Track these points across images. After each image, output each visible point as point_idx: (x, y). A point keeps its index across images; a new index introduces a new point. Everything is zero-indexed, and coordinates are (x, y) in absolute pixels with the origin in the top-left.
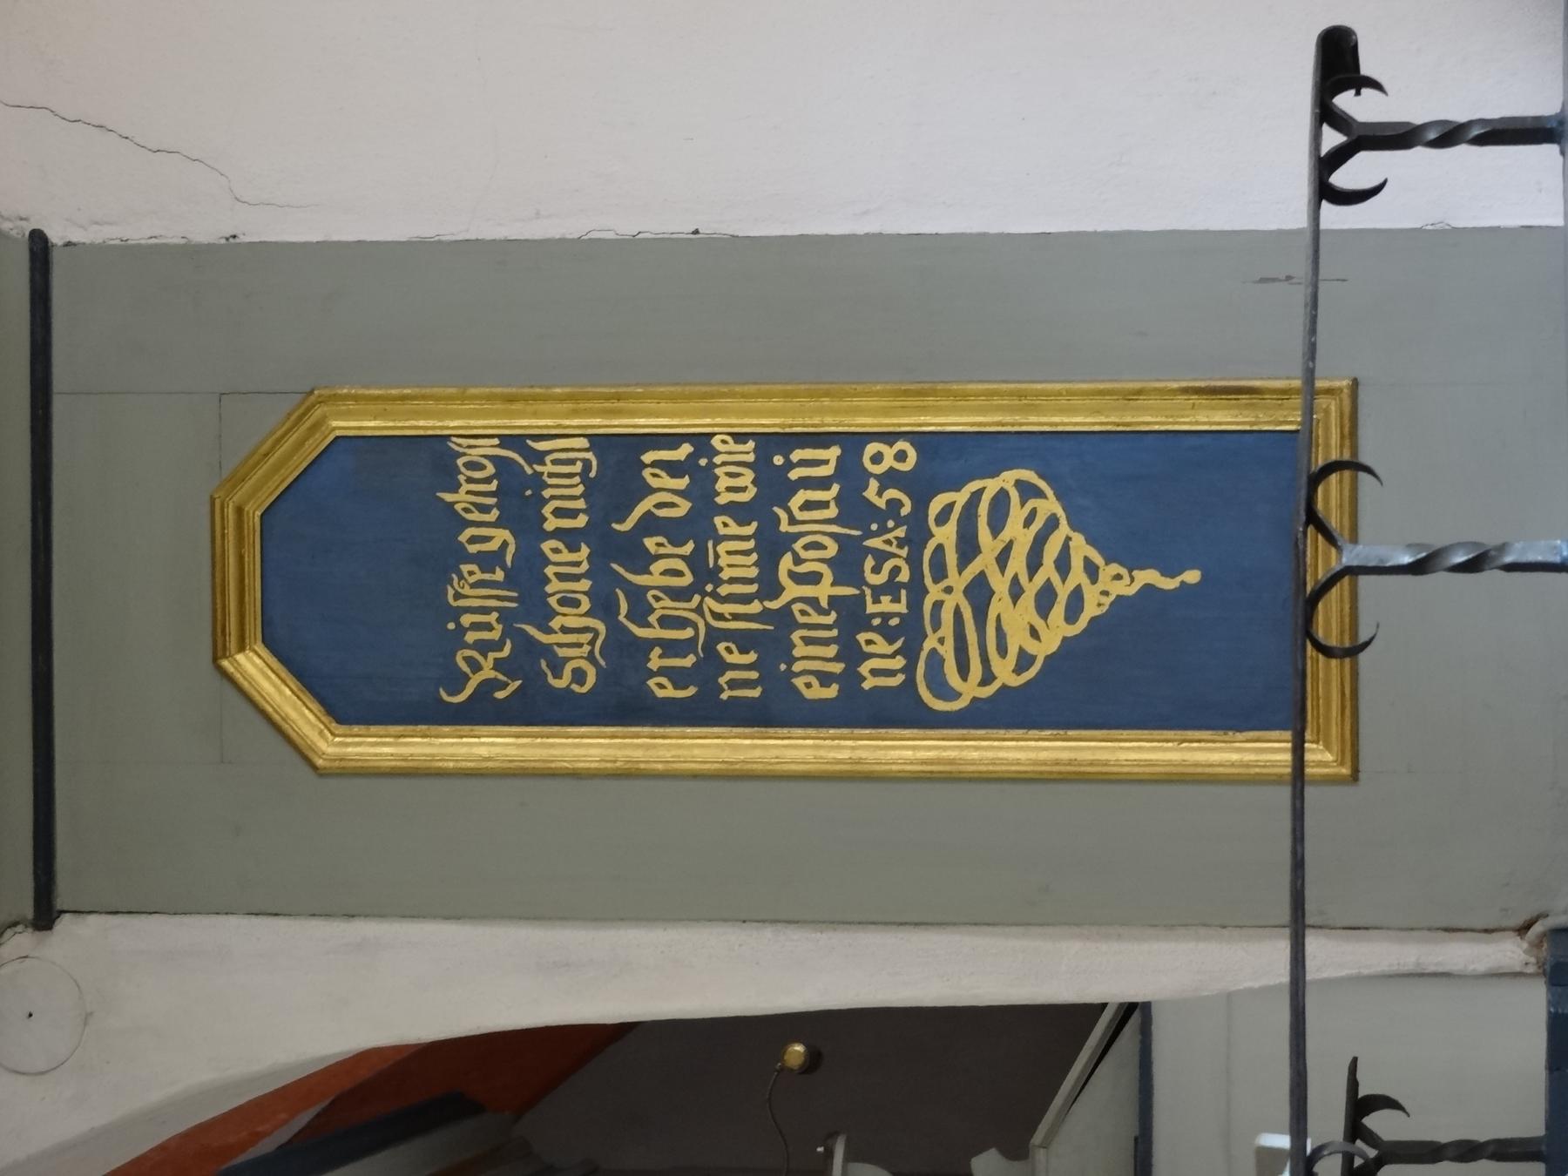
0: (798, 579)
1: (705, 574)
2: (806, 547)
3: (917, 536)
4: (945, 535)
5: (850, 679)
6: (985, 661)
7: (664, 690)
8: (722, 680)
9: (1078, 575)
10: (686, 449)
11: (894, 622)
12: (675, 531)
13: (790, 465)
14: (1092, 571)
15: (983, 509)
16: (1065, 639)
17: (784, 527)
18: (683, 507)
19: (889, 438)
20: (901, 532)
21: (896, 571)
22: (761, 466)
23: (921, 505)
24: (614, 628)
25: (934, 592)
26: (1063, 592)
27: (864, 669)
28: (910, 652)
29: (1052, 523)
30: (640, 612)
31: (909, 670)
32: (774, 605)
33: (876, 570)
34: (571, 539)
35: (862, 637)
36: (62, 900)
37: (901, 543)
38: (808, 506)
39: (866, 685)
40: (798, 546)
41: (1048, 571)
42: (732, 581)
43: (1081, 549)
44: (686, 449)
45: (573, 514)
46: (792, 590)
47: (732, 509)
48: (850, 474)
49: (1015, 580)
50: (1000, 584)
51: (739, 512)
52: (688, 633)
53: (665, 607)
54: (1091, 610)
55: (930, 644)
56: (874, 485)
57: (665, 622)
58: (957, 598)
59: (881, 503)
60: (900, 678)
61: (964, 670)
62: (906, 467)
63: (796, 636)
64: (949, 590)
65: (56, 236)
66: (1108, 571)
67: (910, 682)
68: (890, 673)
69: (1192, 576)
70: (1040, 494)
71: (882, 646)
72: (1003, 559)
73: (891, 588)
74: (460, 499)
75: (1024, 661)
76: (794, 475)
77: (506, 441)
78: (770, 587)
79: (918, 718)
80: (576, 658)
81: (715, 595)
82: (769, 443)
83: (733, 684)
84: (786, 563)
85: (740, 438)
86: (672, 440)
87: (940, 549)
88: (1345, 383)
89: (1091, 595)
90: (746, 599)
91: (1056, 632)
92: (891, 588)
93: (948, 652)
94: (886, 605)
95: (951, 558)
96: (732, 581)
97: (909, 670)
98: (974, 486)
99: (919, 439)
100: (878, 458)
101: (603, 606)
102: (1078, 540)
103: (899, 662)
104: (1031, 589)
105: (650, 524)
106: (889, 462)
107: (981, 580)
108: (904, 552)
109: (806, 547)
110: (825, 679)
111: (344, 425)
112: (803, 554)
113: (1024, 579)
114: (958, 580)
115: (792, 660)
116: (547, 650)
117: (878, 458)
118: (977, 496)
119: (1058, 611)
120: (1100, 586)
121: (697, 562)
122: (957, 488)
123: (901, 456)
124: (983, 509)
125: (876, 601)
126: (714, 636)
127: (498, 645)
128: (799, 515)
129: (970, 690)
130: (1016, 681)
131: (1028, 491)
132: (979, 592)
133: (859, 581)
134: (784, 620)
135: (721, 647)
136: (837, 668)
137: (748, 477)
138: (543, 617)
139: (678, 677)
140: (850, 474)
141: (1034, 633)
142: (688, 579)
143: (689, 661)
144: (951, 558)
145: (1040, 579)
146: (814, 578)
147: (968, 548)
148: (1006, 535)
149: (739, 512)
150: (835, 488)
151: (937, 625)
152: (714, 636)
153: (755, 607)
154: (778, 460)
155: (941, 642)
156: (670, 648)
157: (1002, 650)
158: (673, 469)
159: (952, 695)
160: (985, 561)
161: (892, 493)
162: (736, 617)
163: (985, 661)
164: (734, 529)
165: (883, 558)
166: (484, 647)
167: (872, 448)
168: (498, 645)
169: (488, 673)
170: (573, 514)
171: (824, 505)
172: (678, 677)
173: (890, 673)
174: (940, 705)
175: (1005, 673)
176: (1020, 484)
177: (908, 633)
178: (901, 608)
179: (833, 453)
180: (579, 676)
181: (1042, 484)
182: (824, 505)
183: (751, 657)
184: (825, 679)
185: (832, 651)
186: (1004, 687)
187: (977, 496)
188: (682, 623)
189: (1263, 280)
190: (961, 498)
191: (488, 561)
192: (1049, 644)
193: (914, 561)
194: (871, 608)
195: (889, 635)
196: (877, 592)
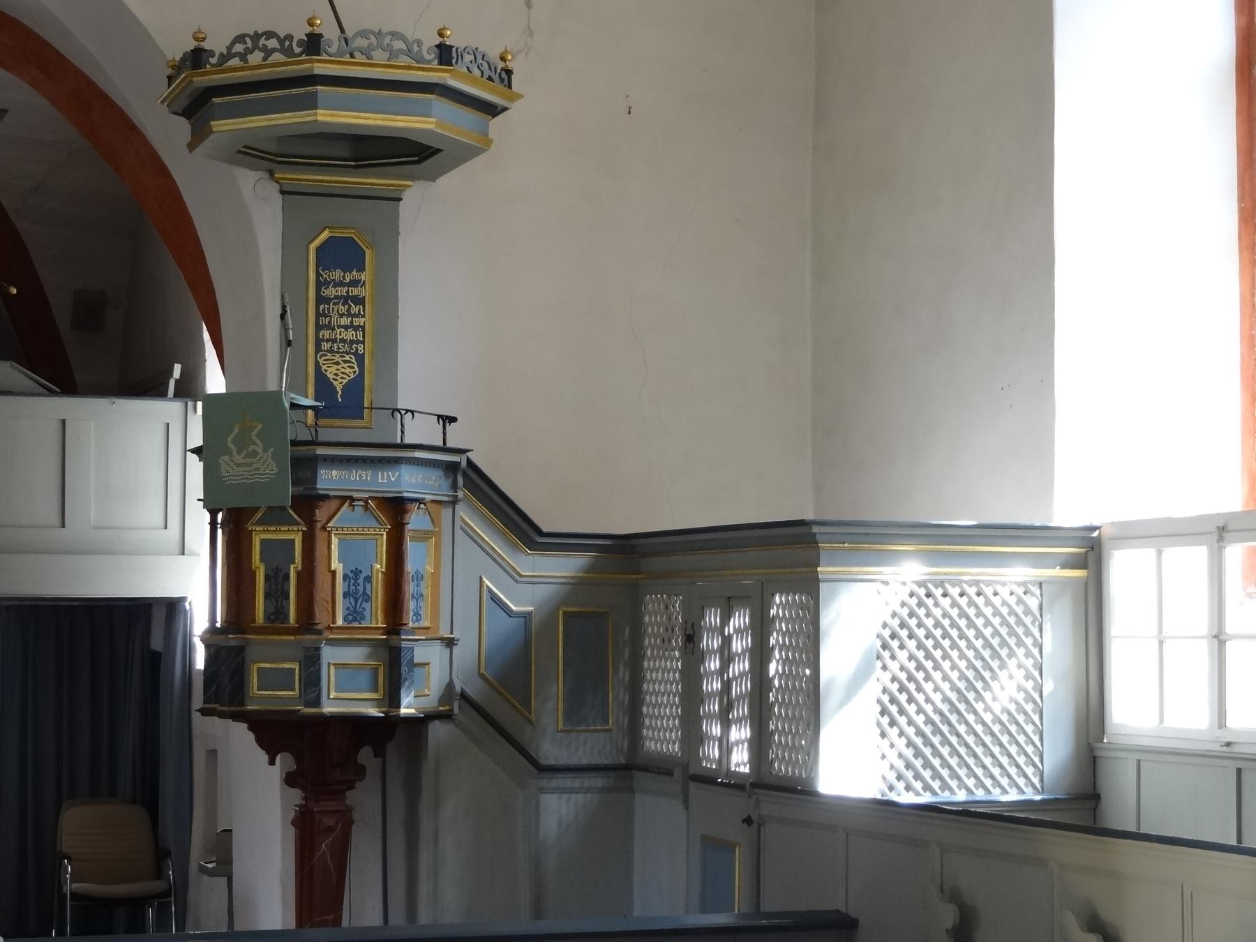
1: (341, 316)
4: (347, 358)
5: (323, 340)
7: (321, 307)
9: (340, 380)
10: (363, 313)
12: (349, 311)
14: (341, 383)
18: (353, 313)
19: (364, 349)
22: (359, 326)
23: (352, 354)
24: (333, 299)
25: (338, 356)
27: (325, 343)
28: (328, 351)
29: (349, 376)
30: (334, 304)
31: (325, 351)
34: (347, 292)
36: (286, 196)
38: (353, 335)
41: (341, 375)
43: (345, 381)
44: (363, 313)
45: (352, 293)
47: (352, 321)
48: (358, 342)
50: (339, 367)
51: (352, 321)
52: (331, 312)
53: (336, 308)
55: (329, 354)
57: (333, 308)
58: (337, 360)
61: (324, 360)
63: (331, 331)
65: (401, 202)
66: (341, 385)
69: (340, 400)
71: (329, 346)
73: (339, 348)
74: (354, 272)
75: (326, 371)
77: (364, 281)
78: (339, 327)
79: (316, 353)
80: (327, 292)
82: (363, 328)
84: (343, 330)
85: (364, 323)
86: (364, 311)
90: (337, 323)
91: (331, 376)
92: (339, 348)
93: (327, 358)
94: (336, 347)
97: (325, 351)
100: (360, 347)
101: (336, 297)
102: (347, 381)
104: (338, 372)
105: (350, 306)
106: (360, 349)
110: (323, 336)
111: (368, 253)
114: (340, 360)
115: (327, 330)
116: (328, 287)
118: (354, 364)
119: (335, 377)
121: (343, 314)
122: (356, 360)
123: (361, 351)
126: (331, 317)
127: (329, 278)
129: (321, 361)
130: (323, 369)
131: (355, 372)
132: (337, 363)
134: (333, 329)
138: (334, 286)
139: (324, 310)
140: (358, 342)
142: (340, 313)
143: (326, 312)
146: (340, 335)
147: (345, 362)
148: (347, 368)
149: (352, 321)
152: (331, 317)
153: (336, 324)
155: (329, 356)
156: (329, 309)
157: (328, 367)
158: (359, 311)
159: (320, 358)
160: (343, 365)
164: (349, 321)
165: (344, 347)
166: (329, 276)
167: (362, 346)
168: (329, 278)
169: (325, 276)
170: (352, 293)
172: (324, 310)
174: (318, 356)
175: (324, 367)
177: (331, 351)
178: (335, 350)
179: (361, 339)
180: (324, 292)
184: (323, 336)
187: (354, 364)
188: (333, 311)
190: (354, 361)
191: (344, 279)
192: (328, 374)
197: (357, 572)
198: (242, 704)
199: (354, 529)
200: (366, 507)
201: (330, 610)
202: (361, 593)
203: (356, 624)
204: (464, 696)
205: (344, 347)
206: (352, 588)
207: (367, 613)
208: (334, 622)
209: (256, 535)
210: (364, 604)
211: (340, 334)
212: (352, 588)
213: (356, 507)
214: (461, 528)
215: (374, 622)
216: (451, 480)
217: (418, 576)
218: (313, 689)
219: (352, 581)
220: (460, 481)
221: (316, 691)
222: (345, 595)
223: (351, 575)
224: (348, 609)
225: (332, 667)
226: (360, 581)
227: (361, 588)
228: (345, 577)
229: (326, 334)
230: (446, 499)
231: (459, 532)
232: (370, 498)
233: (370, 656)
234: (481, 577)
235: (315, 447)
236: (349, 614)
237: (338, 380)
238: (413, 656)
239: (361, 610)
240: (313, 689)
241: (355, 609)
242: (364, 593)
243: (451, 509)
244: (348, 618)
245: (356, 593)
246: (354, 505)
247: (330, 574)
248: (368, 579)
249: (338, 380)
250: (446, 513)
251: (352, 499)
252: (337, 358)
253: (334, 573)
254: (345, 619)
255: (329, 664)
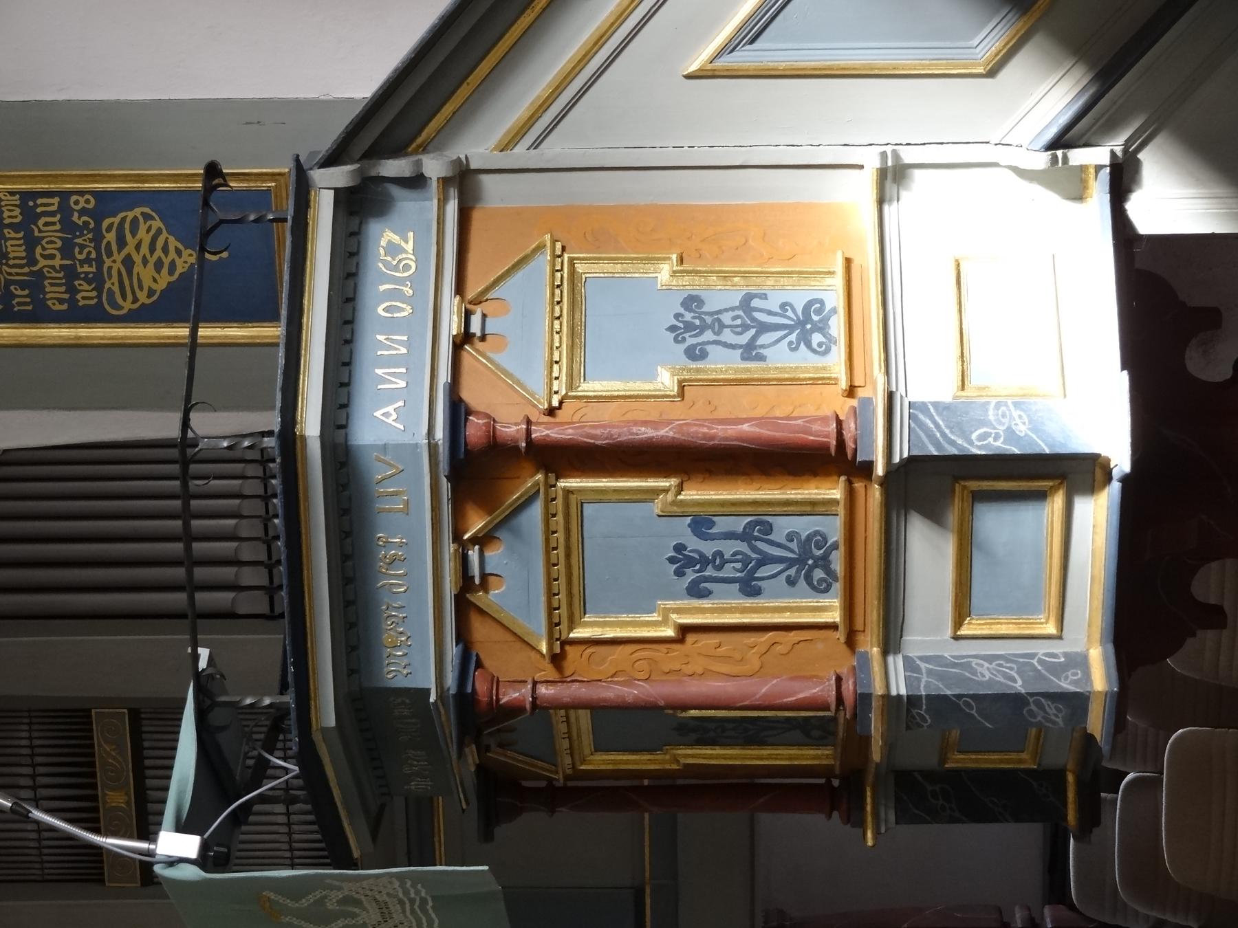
0: (44, 257)
2: (47, 243)
3: (98, 238)
4: (111, 237)
5: (73, 301)
6: (134, 293)
8: (14, 302)
9: (172, 254)
11: (91, 276)
13: (36, 206)
14: (179, 252)
15: (127, 226)
16: (169, 283)
17: (36, 234)
19: (81, 193)
20: (90, 236)
21: (89, 253)
22: (23, 206)
23: (98, 224)
25: (108, 263)
26: (167, 262)
27: (79, 297)
28: (99, 289)
29: (159, 231)
31: (99, 297)
32: (35, 269)
33: (80, 253)
35: (76, 283)
37: (91, 240)
38: (46, 224)
39: (80, 304)
40: (44, 242)
41: (159, 253)
42: (15, 258)
46: (42, 262)
47: (10, 226)
48: (64, 209)
49: (144, 256)
50: (137, 259)
51: (15, 227)
54: (180, 269)
55: (107, 286)
56: (76, 214)
58: (118, 265)
59: (80, 223)
60: (96, 300)
61: (124, 297)
62: (91, 206)
63: (46, 283)
64: (114, 261)
67: (100, 302)
68: (91, 298)
70: (152, 218)
71: (86, 287)
72: (138, 247)
73: (88, 261)
75: (151, 292)
76: (39, 210)
78: (32, 261)
81: (7, 264)
82: (26, 196)
83: (19, 304)
84: (39, 250)
85: (12, 193)
87: (109, 243)
88: (286, 168)
89: (179, 262)
91: (164, 280)
92: (88, 261)
93: (116, 288)
94: (86, 268)
95: (114, 247)
96: (15, 258)
97: (99, 297)
98: (122, 215)
99: (95, 193)
100: (76, 203)
102: (172, 239)
103: (94, 294)
104: (152, 261)
106: (82, 204)
107: (129, 256)
108: (92, 245)
109: (47, 243)
110: (61, 301)
112: (46, 246)
113: (148, 256)
114: (119, 257)
117: (76, 203)
118: (124, 219)
119: (165, 271)
120: (183, 259)
122: (115, 216)
123: (87, 201)
124: (127, 226)
125: (82, 267)
128: (43, 229)
129: (128, 305)
130: (148, 301)
131: (147, 217)
132: (128, 262)
133: (73, 258)
135: (12, 288)
136: (66, 296)
137: (17, 212)
140: (64, 209)
141: (155, 280)
144: (114, 247)
145: (155, 256)
146: (52, 257)
147: (122, 243)
148: (139, 236)
149: (15, 227)
150: (59, 216)
151: (110, 277)
152: (8, 283)
153: (26, 270)
154: (31, 203)
155: (112, 284)
157: (141, 288)
159: (120, 308)
160: (130, 248)
161: (85, 218)
162: (18, 274)
163: (134, 293)
164: (13, 235)
165: (82, 247)
171: (53, 224)
173: (91, 298)
174: (114, 312)
175: (143, 297)
176: (142, 213)
177: (98, 281)
178: (93, 269)
179: (56, 200)
181: (154, 214)
182: (53, 224)
183: (26, 292)
184: (61, 301)
185: (63, 289)
186: (143, 304)
187: (124, 219)
189: (247, 123)
190: (117, 220)
192: (162, 284)
193: (97, 249)
194: (79, 270)
195: (89, 282)
196: (82, 262)
197: (682, 560)
198: (1056, 777)
199: (557, 299)
200: (484, 540)
201: (793, 636)
202: (742, 547)
203: (838, 562)
204: (1053, 145)
205: (82, 247)
206: (729, 571)
207: (805, 526)
208: (833, 627)
209: (583, 761)
210: (778, 536)
211: (50, 260)
212: (729, 571)
213: (488, 571)
214: (536, 144)
215: (829, 281)
216: (395, 191)
217: (689, 327)
218: (1033, 707)
219: (710, 572)
220: (393, 167)
221: (1038, 704)
222: (750, 588)
223: (691, 575)
224: (791, 582)
225: (964, 631)
226: (708, 548)
227: (730, 548)
228: (696, 591)
229: (54, 294)
230: (452, 208)
231: (556, 150)
232: (457, 537)
233: (934, 515)
234: (688, 77)
235: (317, 737)
236: (808, 579)
237: (173, 260)
238: (936, 405)
239: (794, 545)
240: (1033, 707)
241: (790, 563)
242: (745, 536)
243: (485, 178)
244: (821, 580)
245: (746, 561)
246: (484, 576)
247: (690, 638)
248: (701, 523)
249: (173, 260)
250: (495, 191)
251: (466, 584)
252: (114, 264)
253: (685, 630)
254: (822, 589)
255: (956, 638)
